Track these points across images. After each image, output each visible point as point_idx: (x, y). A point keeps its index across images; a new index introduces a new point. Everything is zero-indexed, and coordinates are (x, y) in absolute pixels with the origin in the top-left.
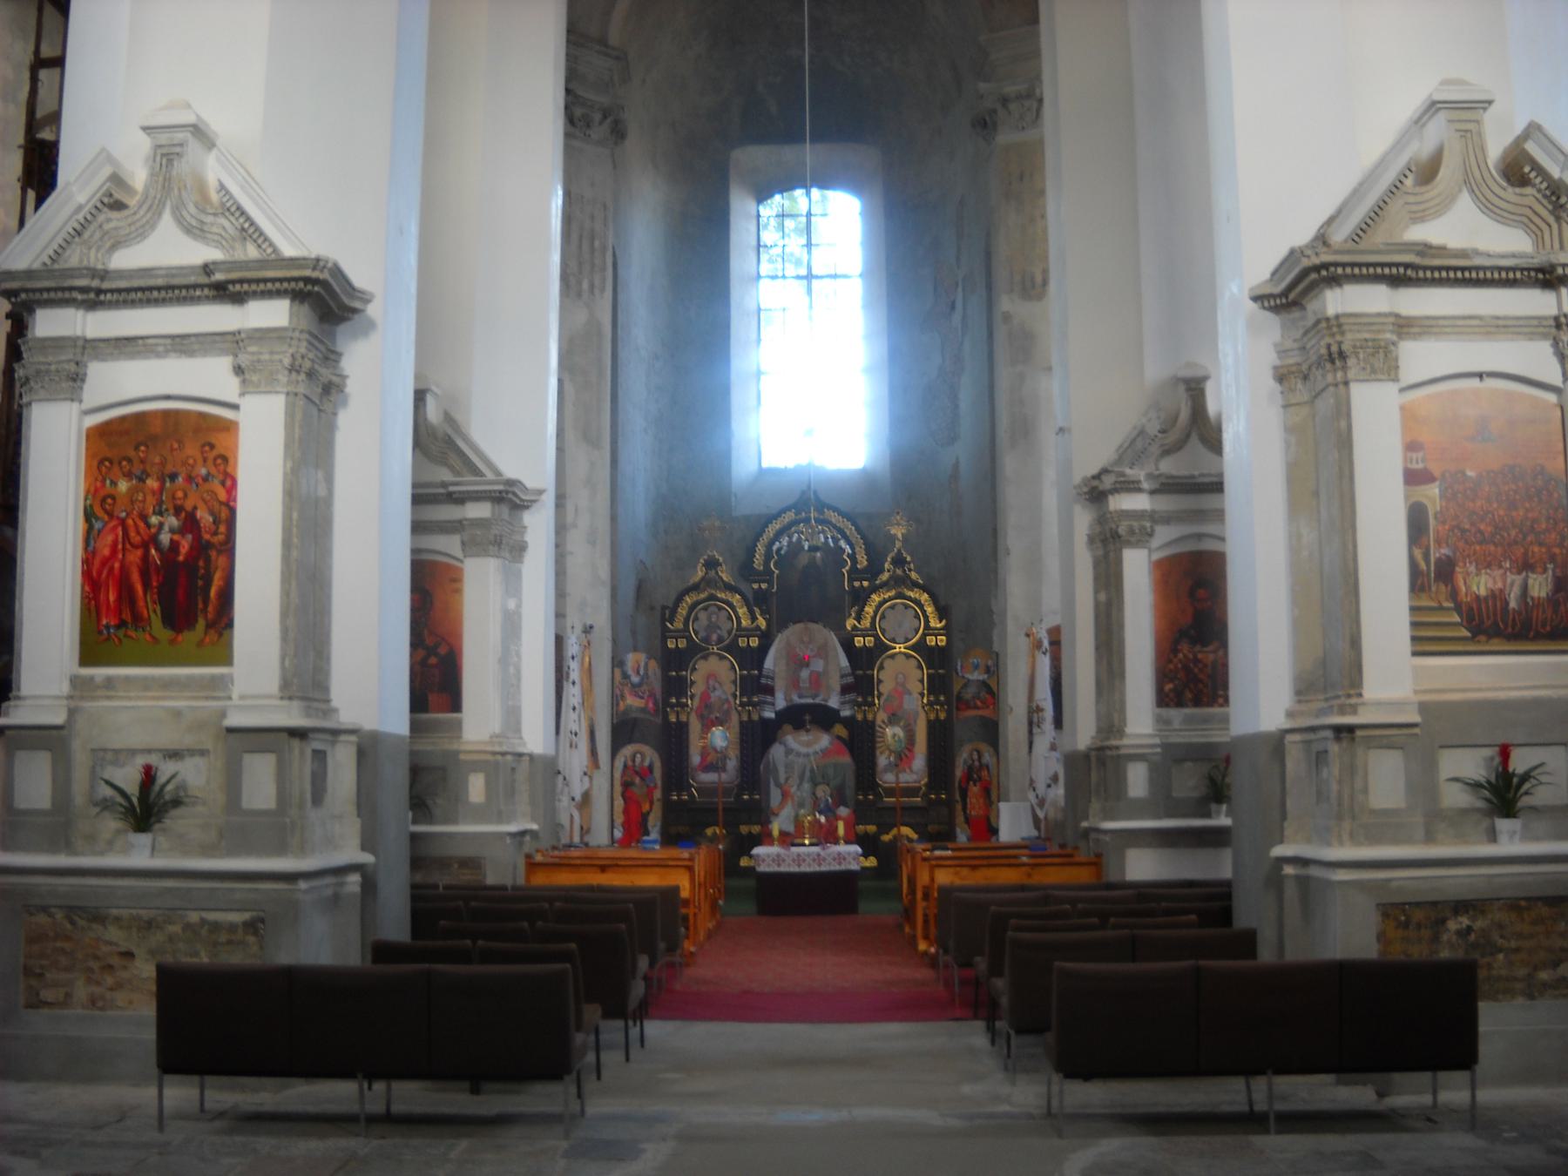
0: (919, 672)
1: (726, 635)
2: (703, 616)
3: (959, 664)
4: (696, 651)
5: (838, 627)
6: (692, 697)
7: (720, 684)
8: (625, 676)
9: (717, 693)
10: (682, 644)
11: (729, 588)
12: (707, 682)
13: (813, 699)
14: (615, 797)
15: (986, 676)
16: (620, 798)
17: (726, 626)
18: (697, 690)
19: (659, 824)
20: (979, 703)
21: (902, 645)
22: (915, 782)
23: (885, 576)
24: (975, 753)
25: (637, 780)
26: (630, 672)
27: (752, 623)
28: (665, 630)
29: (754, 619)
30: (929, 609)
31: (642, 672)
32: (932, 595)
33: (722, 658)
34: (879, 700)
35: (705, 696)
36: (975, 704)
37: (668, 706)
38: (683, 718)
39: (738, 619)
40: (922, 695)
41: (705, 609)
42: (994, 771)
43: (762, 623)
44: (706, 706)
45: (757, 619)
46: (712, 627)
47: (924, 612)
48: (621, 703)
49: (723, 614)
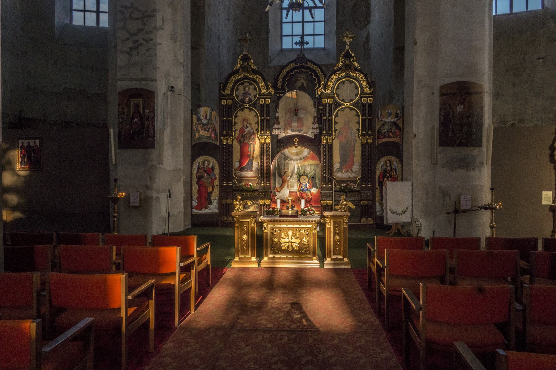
0: (357, 117)
1: (253, 98)
2: (241, 88)
3: (380, 113)
4: (238, 106)
5: (312, 94)
6: (235, 131)
7: (249, 124)
8: (199, 119)
9: (248, 129)
10: (230, 102)
11: (254, 72)
12: (243, 123)
13: (299, 133)
14: (193, 184)
15: (396, 119)
16: (196, 185)
17: (253, 93)
18: (238, 127)
19: (217, 198)
20: (391, 134)
21: (348, 104)
22: (354, 178)
23: (340, 64)
24: (388, 162)
25: (206, 175)
26: (202, 118)
27: (267, 91)
28: (221, 95)
29: (268, 89)
30: (364, 83)
31: (208, 118)
32: (365, 76)
33: (251, 110)
34: (335, 133)
35: (242, 131)
36: (389, 135)
37: (222, 136)
38: (230, 142)
39: (260, 89)
40: (358, 130)
41: (242, 84)
42: (399, 172)
43: (272, 91)
44: (243, 136)
45: (270, 89)
46: (246, 94)
47: (361, 85)
48: (197, 134)
49: (252, 87)
